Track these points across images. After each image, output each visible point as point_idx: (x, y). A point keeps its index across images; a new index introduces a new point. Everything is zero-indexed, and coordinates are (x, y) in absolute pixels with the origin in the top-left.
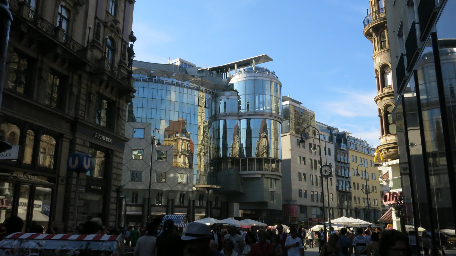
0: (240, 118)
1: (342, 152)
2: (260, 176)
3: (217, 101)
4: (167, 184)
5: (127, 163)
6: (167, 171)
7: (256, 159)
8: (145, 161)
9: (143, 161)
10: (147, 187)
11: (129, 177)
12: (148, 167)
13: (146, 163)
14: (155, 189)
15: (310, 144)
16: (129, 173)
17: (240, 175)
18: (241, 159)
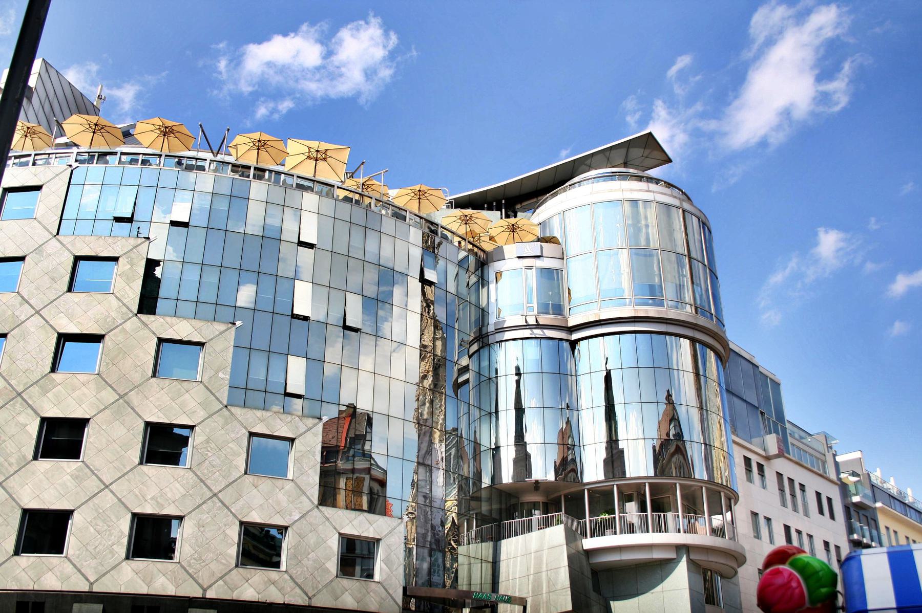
0: (575, 336)
1: (861, 512)
2: (672, 555)
3: (486, 278)
4: (291, 577)
5: (120, 478)
6: (296, 521)
7: (649, 483)
8: (196, 475)
9: (191, 474)
10: (201, 587)
11: (125, 541)
12: (211, 498)
13: (202, 481)
14: (235, 596)
15: (779, 475)
16: (125, 525)
17: (589, 553)
18: (589, 490)
